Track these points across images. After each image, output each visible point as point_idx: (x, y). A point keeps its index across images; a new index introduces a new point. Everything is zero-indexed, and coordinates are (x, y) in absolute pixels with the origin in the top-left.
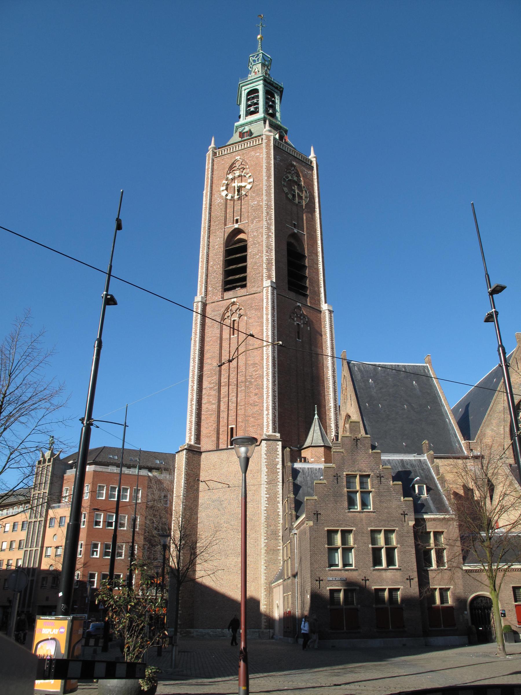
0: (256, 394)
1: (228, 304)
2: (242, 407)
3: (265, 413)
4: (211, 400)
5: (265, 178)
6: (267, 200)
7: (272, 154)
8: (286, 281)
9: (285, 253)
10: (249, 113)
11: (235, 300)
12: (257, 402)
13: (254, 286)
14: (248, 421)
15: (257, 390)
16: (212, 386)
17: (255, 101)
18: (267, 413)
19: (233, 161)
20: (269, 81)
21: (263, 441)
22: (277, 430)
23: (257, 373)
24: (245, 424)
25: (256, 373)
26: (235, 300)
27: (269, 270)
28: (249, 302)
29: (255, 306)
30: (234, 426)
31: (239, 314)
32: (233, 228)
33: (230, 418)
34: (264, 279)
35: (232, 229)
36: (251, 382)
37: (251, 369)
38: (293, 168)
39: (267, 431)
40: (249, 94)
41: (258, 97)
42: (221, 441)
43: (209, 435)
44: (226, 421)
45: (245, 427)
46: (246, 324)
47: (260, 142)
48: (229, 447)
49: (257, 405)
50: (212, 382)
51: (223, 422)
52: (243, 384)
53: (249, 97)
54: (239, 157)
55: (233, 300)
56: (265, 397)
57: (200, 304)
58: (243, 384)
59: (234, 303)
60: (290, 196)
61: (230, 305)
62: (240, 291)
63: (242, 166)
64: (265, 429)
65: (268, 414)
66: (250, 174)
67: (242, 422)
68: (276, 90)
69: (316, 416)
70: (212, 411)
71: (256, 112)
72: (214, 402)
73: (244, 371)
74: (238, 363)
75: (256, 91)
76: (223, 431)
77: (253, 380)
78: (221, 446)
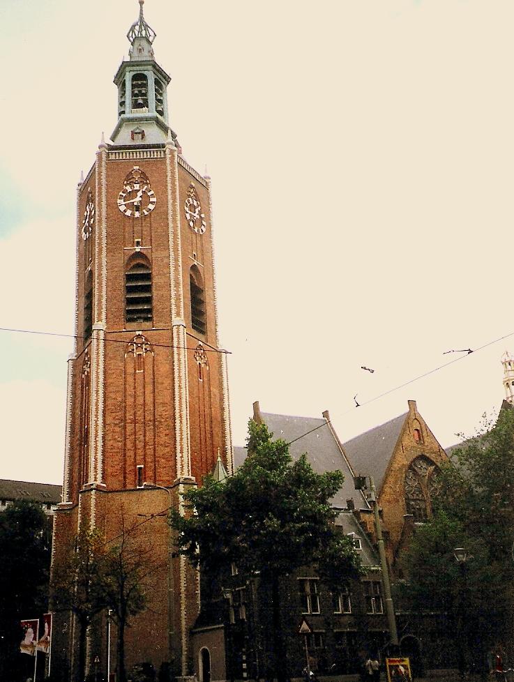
3: (179, 455)
4: (117, 437)
5: (170, 201)
6: (173, 227)
7: (177, 173)
8: (190, 319)
9: (189, 288)
10: (136, 105)
11: (140, 333)
13: (161, 322)
14: (158, 461)
16: (117, 422)
17: (143, 92)
19: (131, 170)
20: (158, 68)
22: (190, 473)
24: (155, 465)
26: (140, 333)
27: (178, 306)
28: (155, 337)
31: (145, 349)
33: (138, 458)
34: (173, 316)
36: (160, 422)
37: (160, 409)
38: (192, 190)
39: (182, 474)
40: (135, 78)
41: (145, 86)
42: (128, 481)
44: (133, 460)
45: (155, 467)
46: (154, 360)
47: (163, 156)
48: (138, 487)
51: (130, 461)
52: (151, 423)
53: (134, 83)
54: (138, 167)
55: (137, 333)
56: (178, 439)
57: (102, 332)
58: (151, 423)
60: (191, 224)
62: (147, 325)
63: (141, 180)
64: (179, 472)
65: (182, 457)
66: (152, 192)
67: (151, 462)
68: (164, 81)
69: (219, 459)
71: (145, 104)
74: (144, 401)
75: (144, 77)
78: (130, 487)
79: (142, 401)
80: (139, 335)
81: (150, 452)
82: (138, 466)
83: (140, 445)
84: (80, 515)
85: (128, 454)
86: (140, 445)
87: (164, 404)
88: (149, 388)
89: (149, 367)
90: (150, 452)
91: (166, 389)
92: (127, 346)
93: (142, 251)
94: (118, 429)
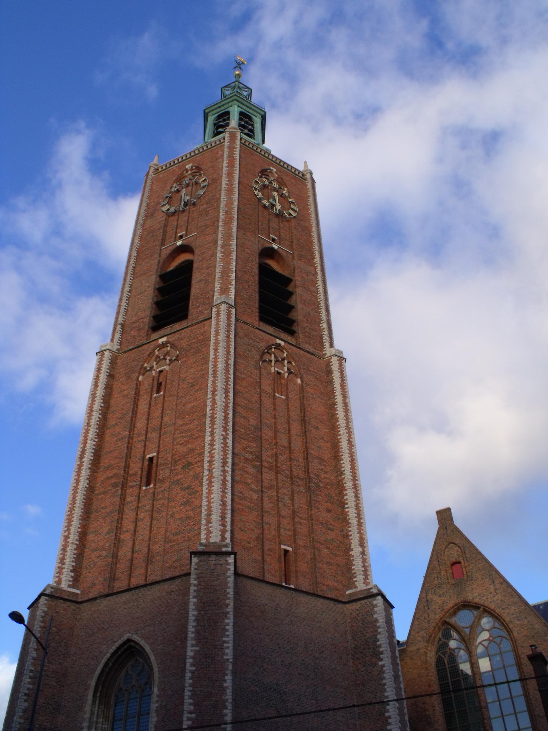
0: (329, 511)
1: (271, 343)
2: (302, 521)
4: (249, 481)
11: (282, 343)
12: (331, 524)
15: (329, 505)
18: (361, 550)
21: (379, 597)
23: (328, 476)
25: (325, 475)
26: (282, 343)
29: (315, 372)
30: (290, 549)
32: (269, 245)
35: (269, 246)
43: (247, 545)
48: (284, 584)
49: (332, 530)
50: (248, 449)
55: (278, 341)
59: (278, 346)
61: (273, 345)
70: (251, 503)
72: (254, 487)
73: (300, 460)
76: (269, 550)
77: (321, 485)
79: (286, 444)
80: (280, 345)
81: (303, 529)
82: (283, 547)
83: (285, 512)
84: (193, 600)
85: (266, 518)
86: (285, 512)
87: (321, 460)
88: (296, 428)
89: (294, 396)
90: (303, 529)
91: (322, 438)
92: (264, 353)
93: (281, 251)
94: (252, 470)
